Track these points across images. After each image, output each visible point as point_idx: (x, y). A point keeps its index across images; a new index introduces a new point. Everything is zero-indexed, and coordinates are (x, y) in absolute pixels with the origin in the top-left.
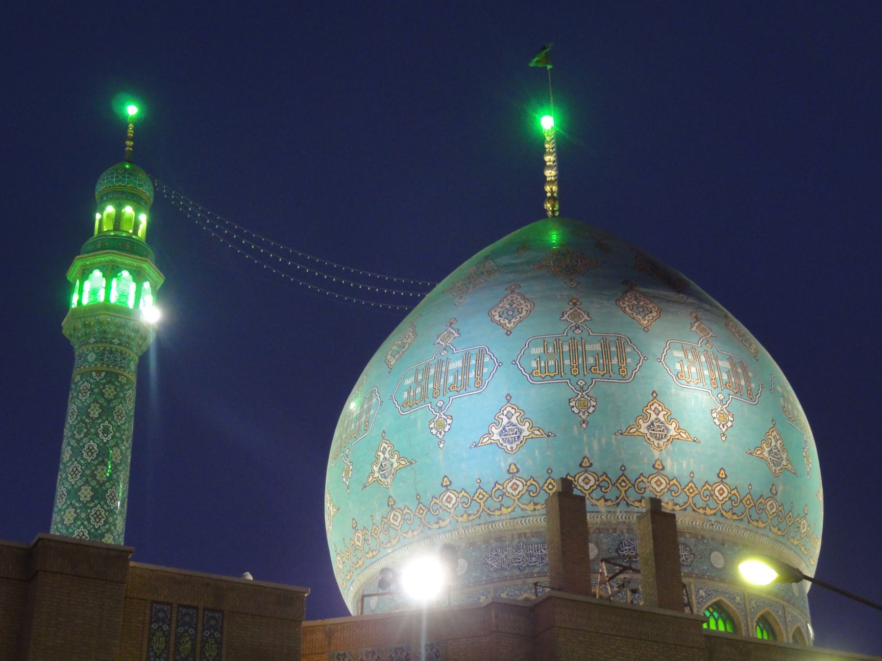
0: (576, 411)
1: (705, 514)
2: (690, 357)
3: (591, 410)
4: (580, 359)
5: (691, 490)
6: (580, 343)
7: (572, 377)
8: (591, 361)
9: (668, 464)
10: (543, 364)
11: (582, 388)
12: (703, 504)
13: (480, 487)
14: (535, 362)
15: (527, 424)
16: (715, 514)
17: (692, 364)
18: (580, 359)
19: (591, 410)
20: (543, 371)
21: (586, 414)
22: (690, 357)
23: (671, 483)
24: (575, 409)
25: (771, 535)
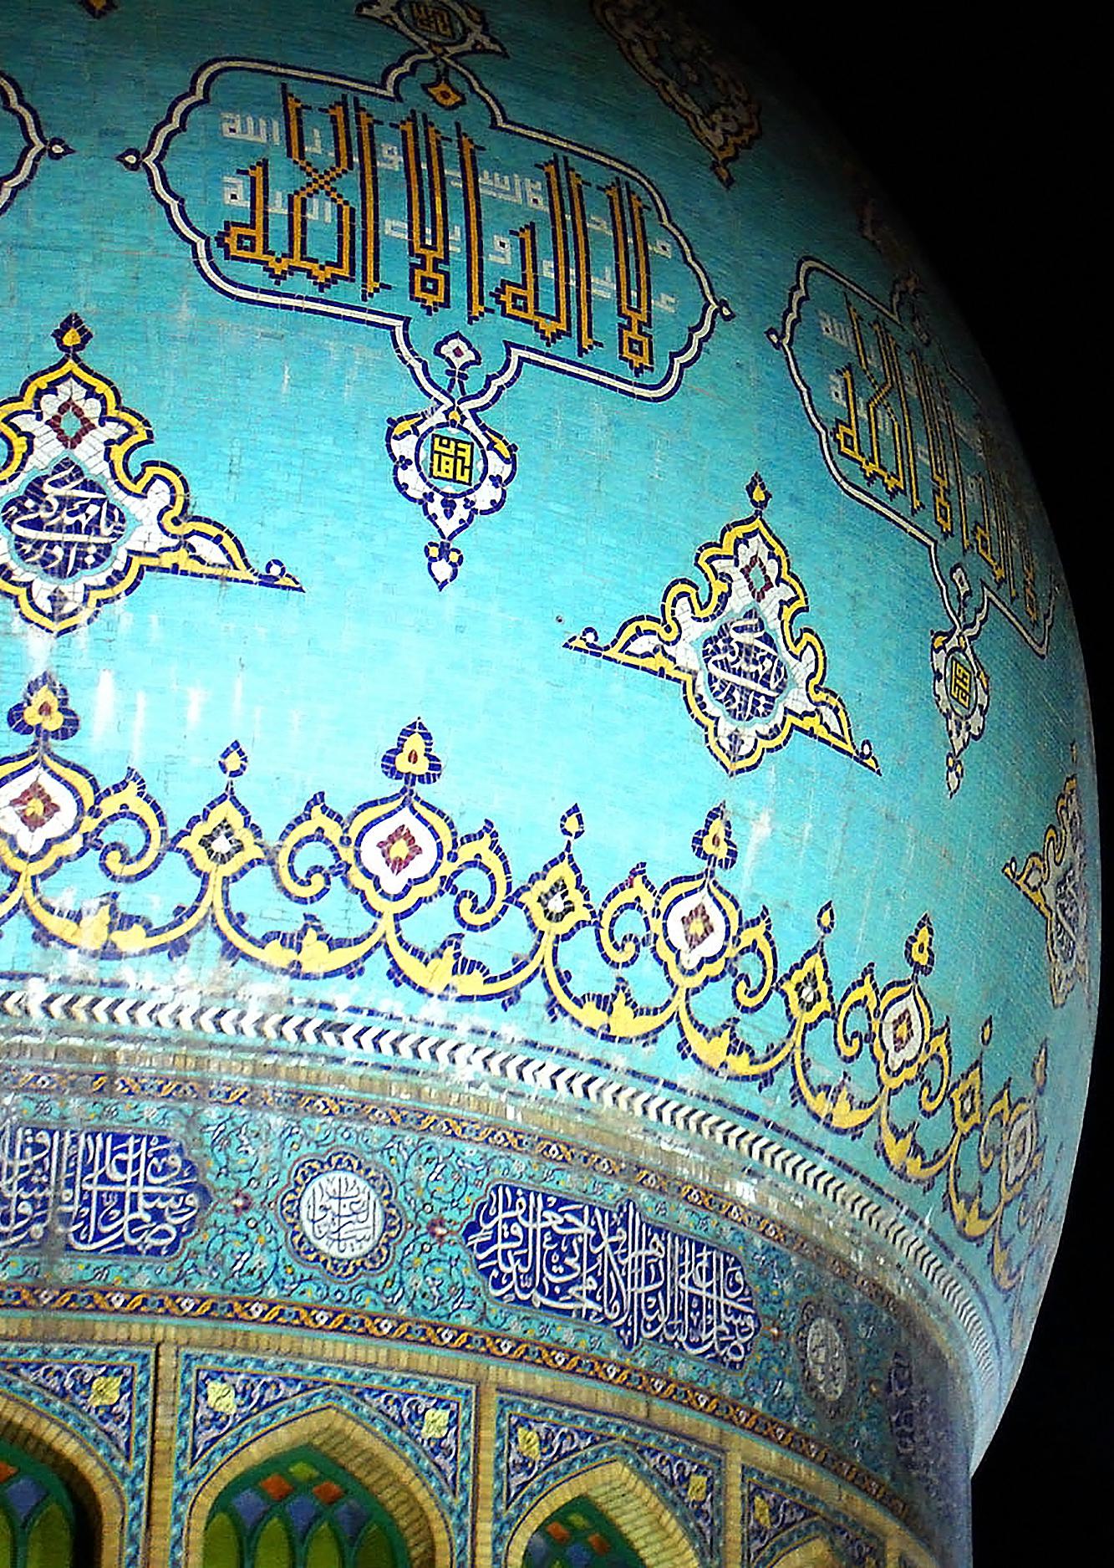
0: (417, 488)
1: (296, 971)
2: (317, 146)
3: (485, 495)
4: (456, 234)
5: (221, 845)
6: (449, 149)
7: (414, 310)
8: (502, 256)
9: (98, 706)
10: (278, 207)
11: (458, 376)
12: (291, 918)
13: (229, 796)
14: (241, 186)
15: (159, 495)
16: (352, 971)
17: (320, 182)
18: (456, 234)
19: (485, 495)
20: (278, 244)
21: (461, 512)
22: (317, 146)
23: (110, 806)
24: (409, 476)
25: (688, 1075)
